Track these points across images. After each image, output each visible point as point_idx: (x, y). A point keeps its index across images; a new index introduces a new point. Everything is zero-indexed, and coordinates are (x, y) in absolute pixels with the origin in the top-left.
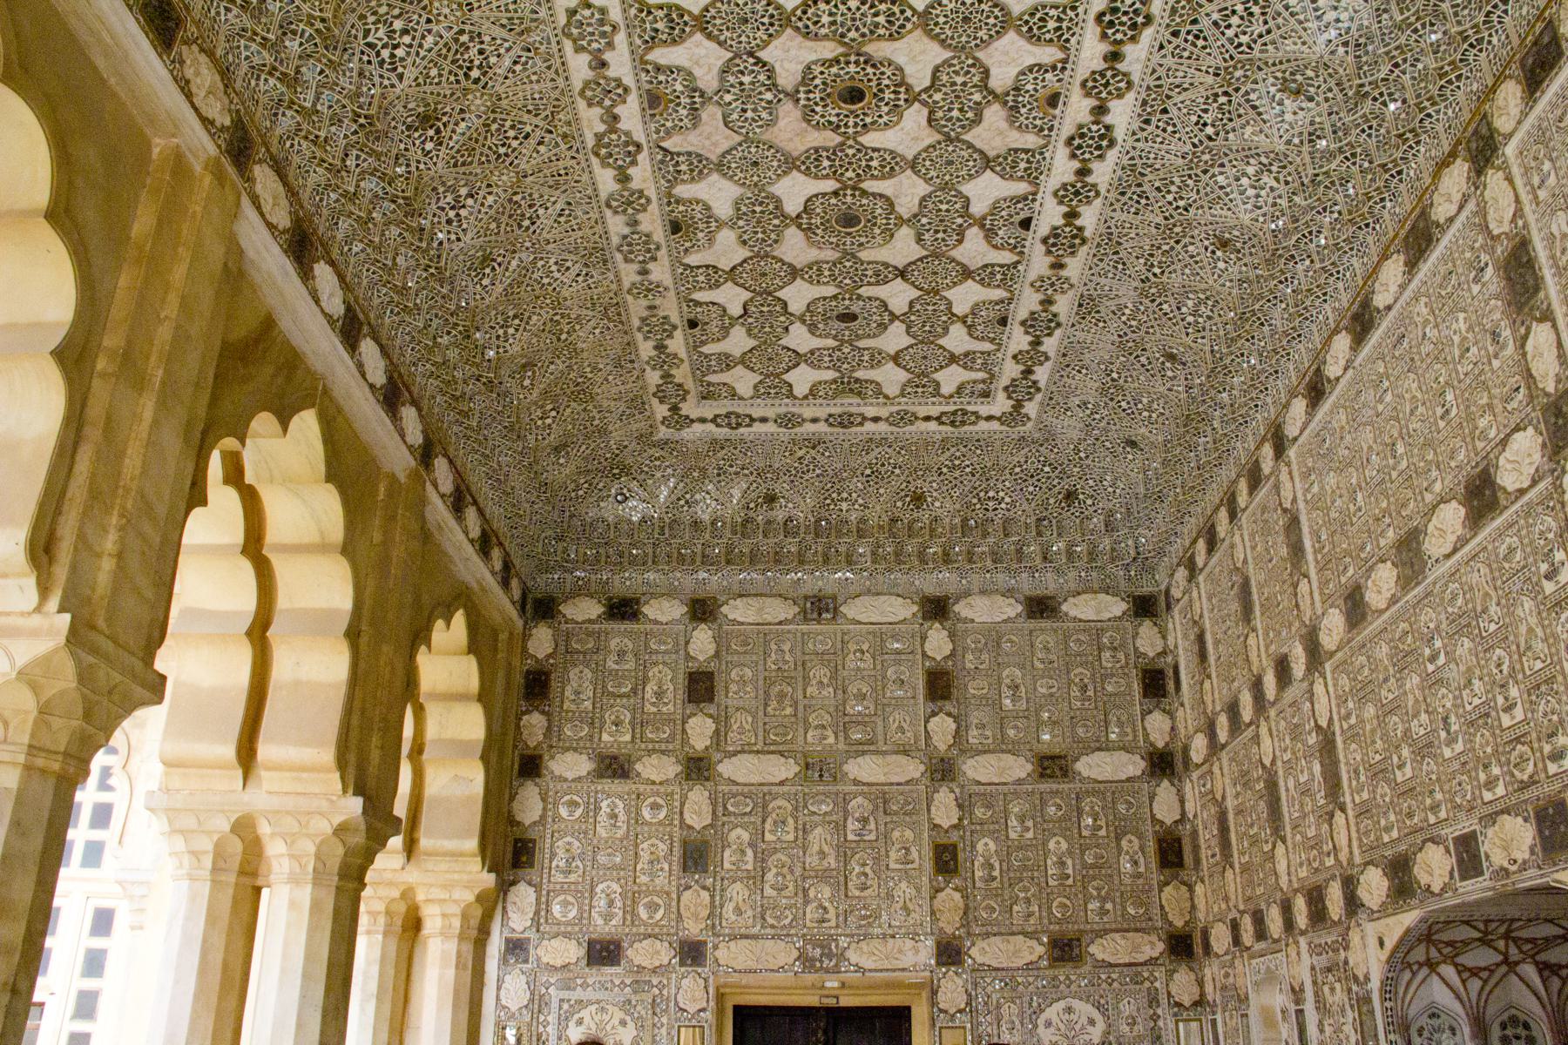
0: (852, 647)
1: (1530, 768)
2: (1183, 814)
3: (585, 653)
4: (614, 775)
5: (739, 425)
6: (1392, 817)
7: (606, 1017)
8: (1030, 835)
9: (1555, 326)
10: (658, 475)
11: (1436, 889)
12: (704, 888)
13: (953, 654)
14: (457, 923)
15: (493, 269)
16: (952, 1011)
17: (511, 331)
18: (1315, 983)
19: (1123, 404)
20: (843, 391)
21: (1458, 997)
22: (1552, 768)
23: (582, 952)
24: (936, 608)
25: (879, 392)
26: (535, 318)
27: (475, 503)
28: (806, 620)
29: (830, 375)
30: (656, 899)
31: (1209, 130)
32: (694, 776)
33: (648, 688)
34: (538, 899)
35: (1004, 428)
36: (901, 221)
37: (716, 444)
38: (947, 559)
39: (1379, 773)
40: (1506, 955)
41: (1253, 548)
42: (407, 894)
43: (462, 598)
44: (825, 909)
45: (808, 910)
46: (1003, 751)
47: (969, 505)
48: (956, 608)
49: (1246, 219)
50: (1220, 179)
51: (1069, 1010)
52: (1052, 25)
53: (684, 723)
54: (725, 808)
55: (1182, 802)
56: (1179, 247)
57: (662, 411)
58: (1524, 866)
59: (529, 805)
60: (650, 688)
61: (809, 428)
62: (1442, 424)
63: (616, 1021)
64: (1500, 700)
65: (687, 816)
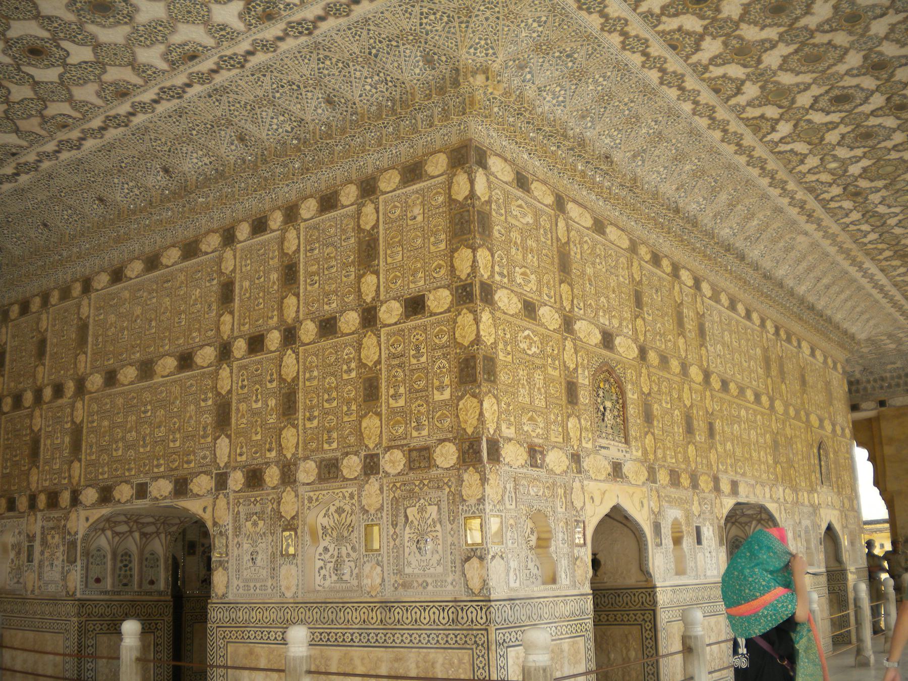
1: (177, 464)
6: (106, 469)
9: (233, 318)
11: (123, 500)
18: (43, 533)
21: (109, 543)
22: (185, 466)
31: (123, 165)
39: (102, 450)
40: (131, 528)
41: (54, 326)
49: (119, 199)
52: (86, 108)
58: (165, 498)
62: (176, 325)
64: (171, 437)
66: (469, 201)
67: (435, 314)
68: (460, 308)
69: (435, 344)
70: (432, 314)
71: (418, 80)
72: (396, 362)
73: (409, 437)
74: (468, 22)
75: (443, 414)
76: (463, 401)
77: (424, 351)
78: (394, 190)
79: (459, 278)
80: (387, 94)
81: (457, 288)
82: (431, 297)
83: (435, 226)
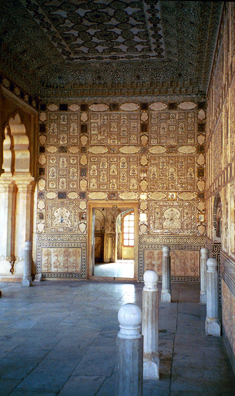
0: (122, 117)
2: (205, 163)
3: (54, 120)
4: (63, 152)
5: (86, 60)
7: (63, 211)
8: (165, 167)
10: (68, 72)
12: (85, 180)
13: (148, 120)
14: (26, 189)
15: (9, 34)
16: (143, 210)
17: (17, 45)
19: (185, 55)
20: (112, 51)
23: (57, 195)
24: (144, 107)
25: (121, 51)
26: (23, 41)
27: (17, 86)
28: (111, 110)
29: (107, 47)
30: (74, 183)
32: (83, 152)
33: (71, 129)
34: (46, 183)
35: (158, 58)
36: (111, 17)
37: (81, 64)
38: (147, 93)
42: (13, 182)
43: (18, 110)
44: (114, 185)
45: (110, 185)
46: (159, 145)
47: (152, 78)
48: (150, 107)
50: (185, 10)
51: (172, 210)
53: (80, 138)
54: (90, 160)
55: (205, 159)
56: (182, 23)
57: (65, 57)
59: (43, 160)
60: (72, 129)
61: (104, 60)
63: (65, 211)
65: (81, 162)
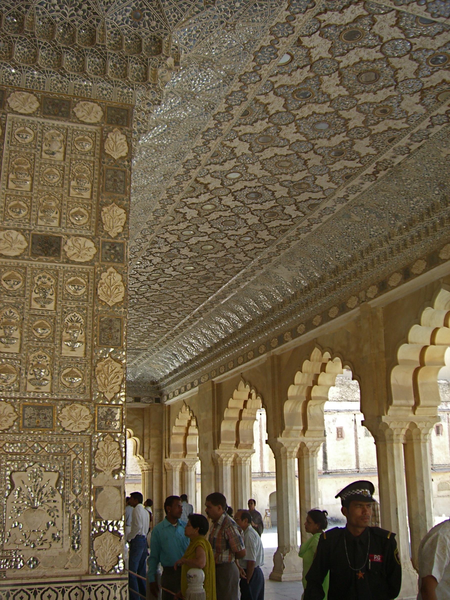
66: (126, 163)
67: (73, 262)
68: (106, 264)
69: (69, 294)
70: (68, 261)
71: (113, 27)
72: (12, 300)
73: (22, 390)
74: (202, 9)
75: (72, 372)
76: (103, 363)
77: (53, 297)
78: (29, 115)
79: (107, 233)
80: (68, 19)
81: (104, 244)
82: (69, 243)
83: (78, 171)
